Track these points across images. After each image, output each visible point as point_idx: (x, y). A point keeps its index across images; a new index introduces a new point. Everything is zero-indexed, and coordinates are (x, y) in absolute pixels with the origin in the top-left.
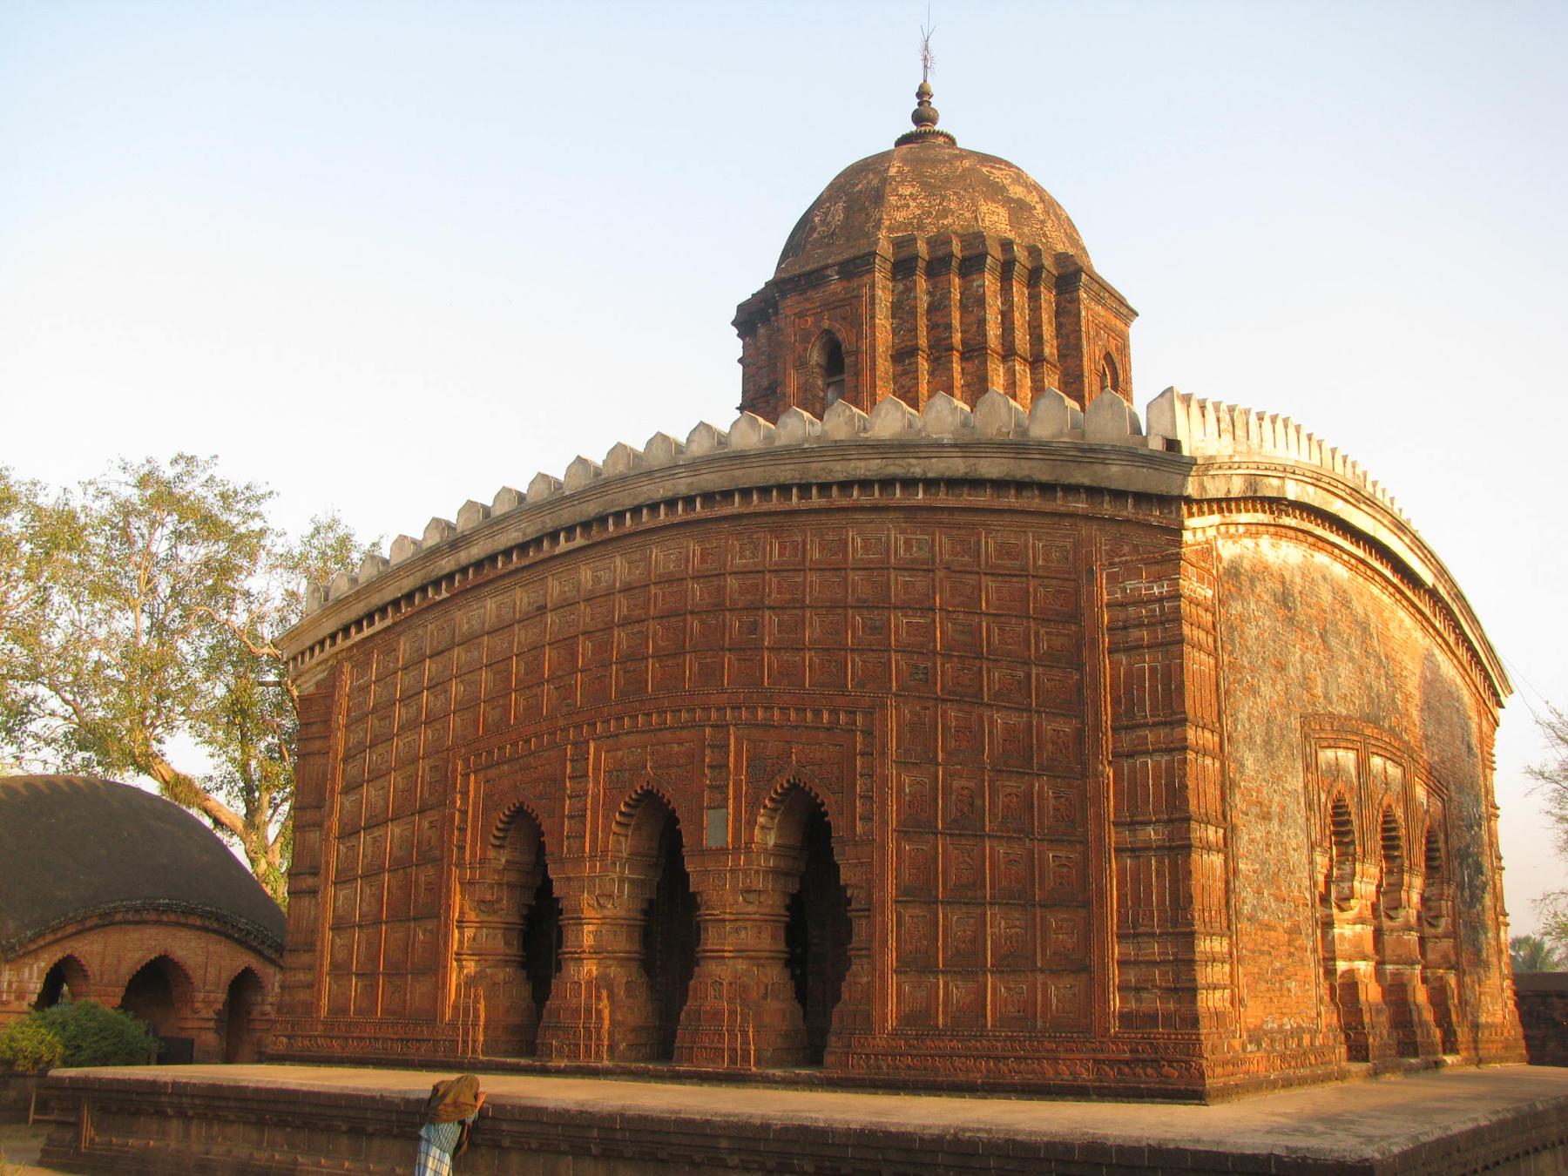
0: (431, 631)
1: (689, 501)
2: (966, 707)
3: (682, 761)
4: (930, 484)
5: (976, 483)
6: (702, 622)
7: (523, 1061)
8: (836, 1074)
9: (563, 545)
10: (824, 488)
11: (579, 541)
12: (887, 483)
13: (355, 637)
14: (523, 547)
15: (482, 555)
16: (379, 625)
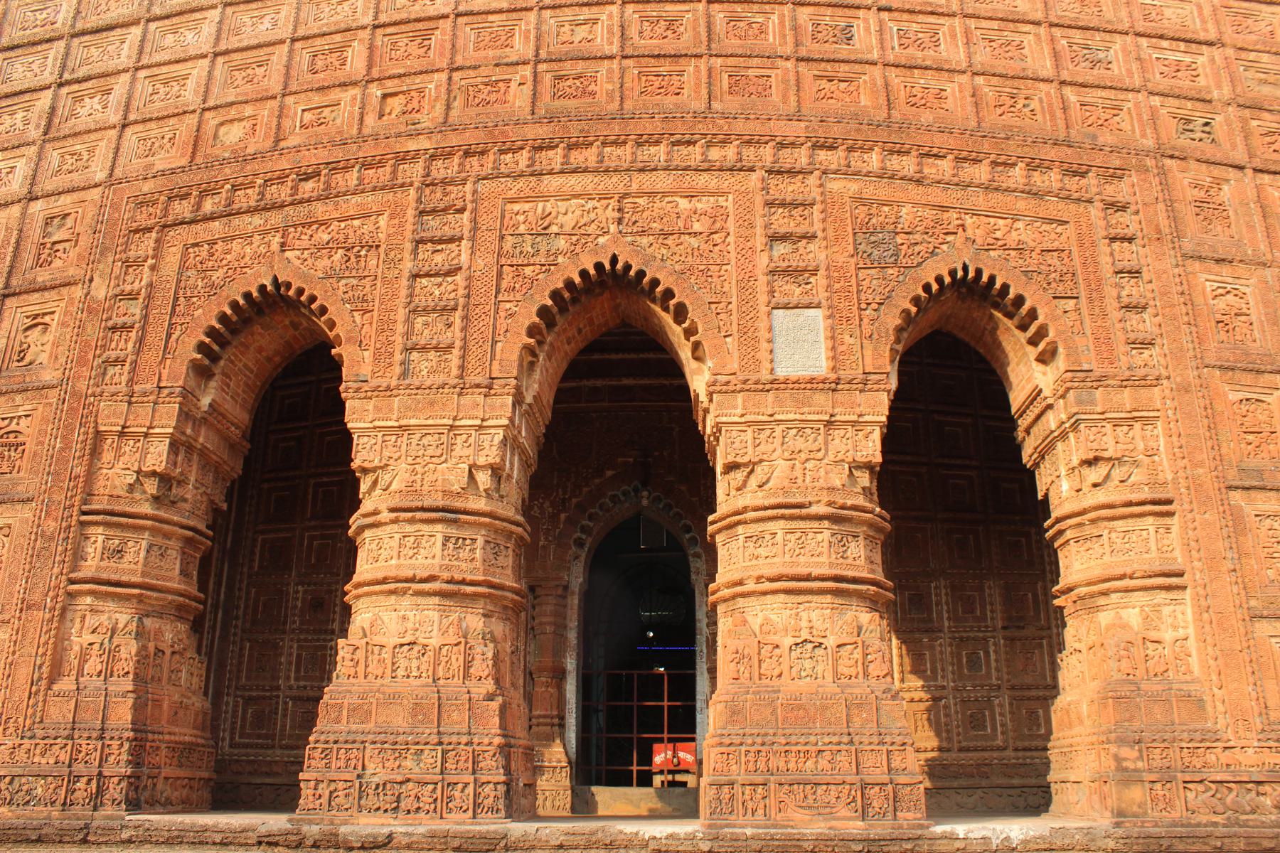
3: (697, 227)
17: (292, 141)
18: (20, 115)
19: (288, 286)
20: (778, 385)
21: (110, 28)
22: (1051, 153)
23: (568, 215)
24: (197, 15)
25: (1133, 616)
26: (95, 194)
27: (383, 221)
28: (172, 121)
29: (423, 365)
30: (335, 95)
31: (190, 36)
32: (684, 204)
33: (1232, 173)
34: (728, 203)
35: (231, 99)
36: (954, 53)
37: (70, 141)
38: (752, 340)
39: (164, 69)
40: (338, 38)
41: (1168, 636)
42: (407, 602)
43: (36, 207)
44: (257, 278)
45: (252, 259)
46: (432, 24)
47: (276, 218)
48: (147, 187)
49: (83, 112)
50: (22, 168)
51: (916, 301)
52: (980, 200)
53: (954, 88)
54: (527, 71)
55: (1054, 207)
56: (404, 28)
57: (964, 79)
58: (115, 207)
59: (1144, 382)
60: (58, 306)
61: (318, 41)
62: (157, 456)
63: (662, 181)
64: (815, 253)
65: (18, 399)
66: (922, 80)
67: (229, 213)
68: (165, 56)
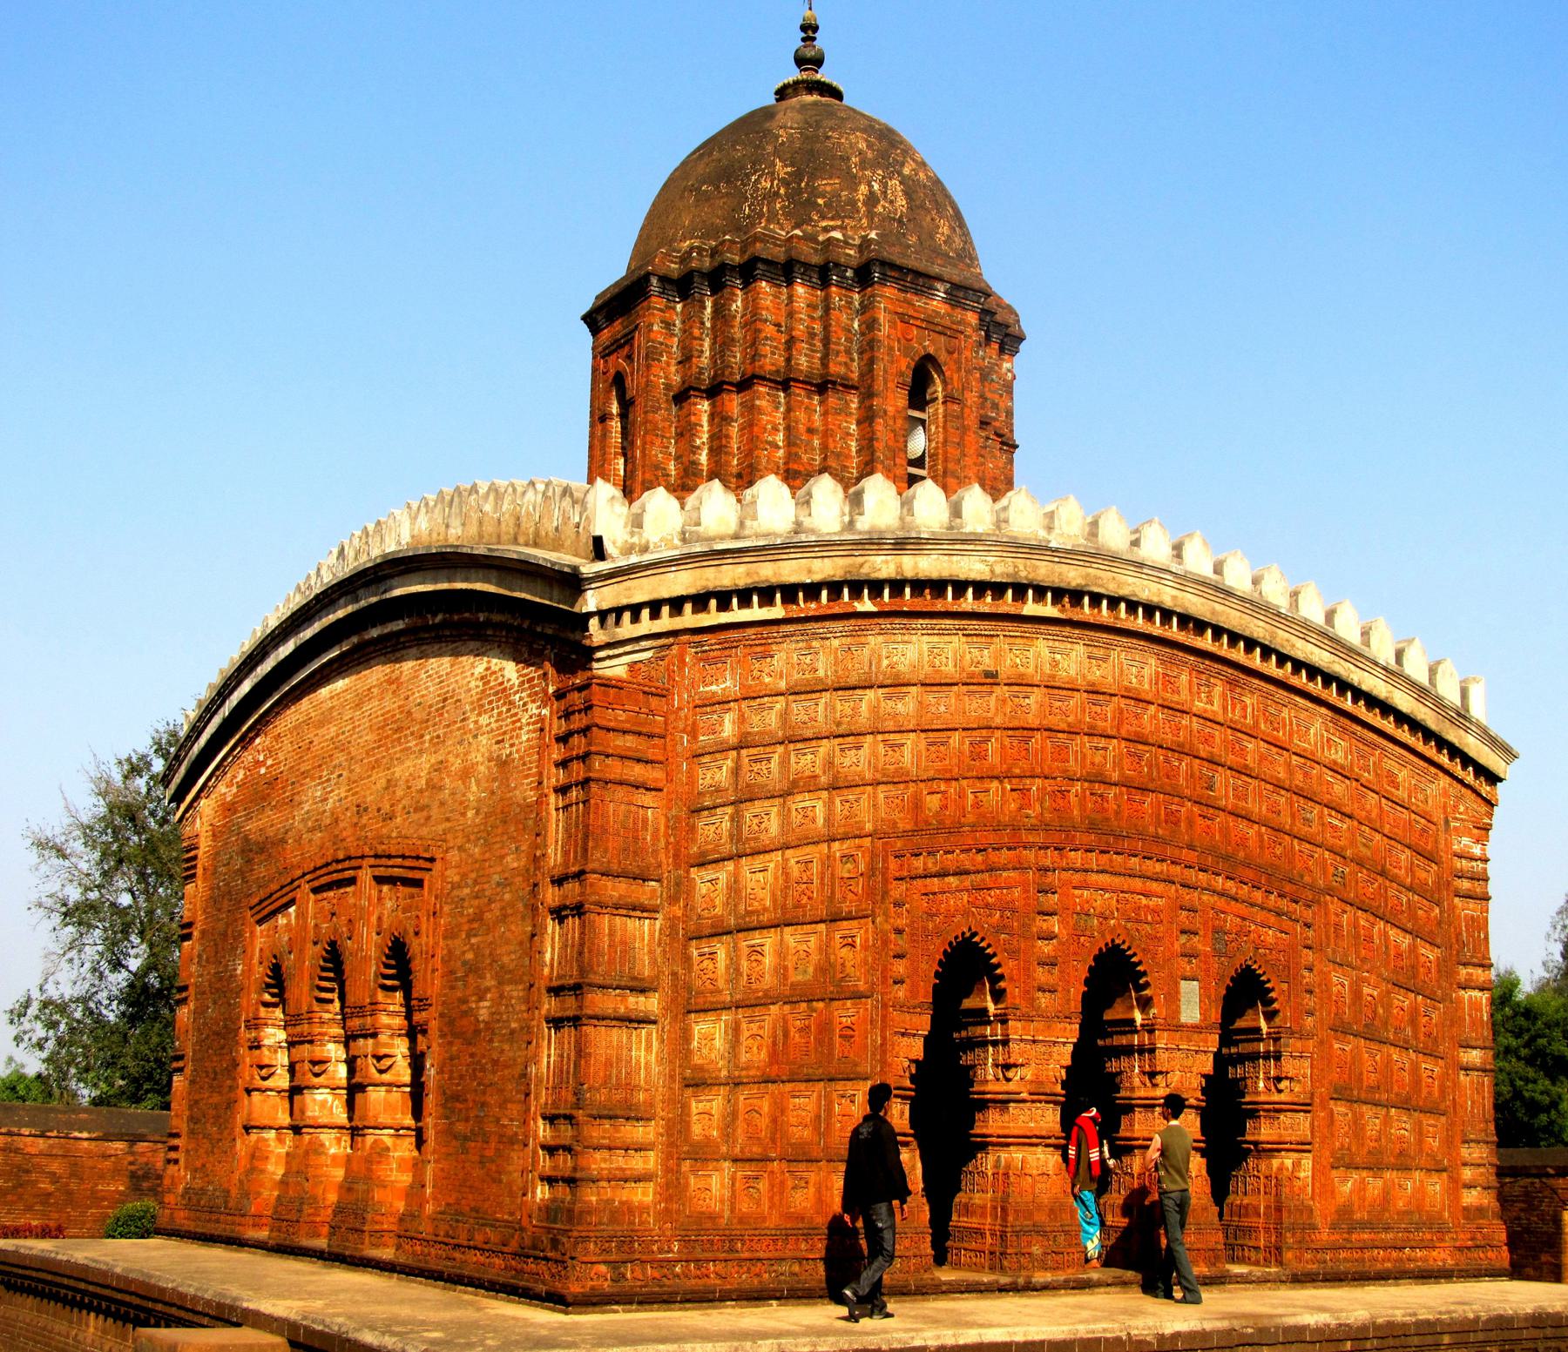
0: (825, 654)
1: (1167, 615)
2: (1371, 918)
4: (1358, 694)
5: (1386, 709)
6: (1167, 761)
7: (986, 1278)
8: (1300, 1268)
9: (1030, 608)
10: (1283, 659)
11: (1048, 610)
12: (1329, 678)
13: (713, 617)
14: (981, 588)
15: (935, 575)
16: (756, 613)
17: (971, 818)
18: (809, 757)
19: (975, 934)
20: (1180, 1027)
21: (854, 688)
22: (1288, 888)
23: (1100, 901)
24: (904, 689)
25: (1288, 1163)
26: (867, 842)
27: (1017, 892)
28: (902, 786)
29: (1044, 1000)
30: (986, 784)
31: (900, 707)
32: (1144, 901)
33: (1348, 908)
34: (1161, 902)
35: (931, 774)
36: (1254, 806)
37: (845, 792)
38: (1173, 997)
39: (892, 736)
40: (984, 732)
41: (1302, 1175)
42: (1040, 1149)
43: (836, 845)
44: (960, 927)
45: (957, 907)
46: (1030, 733)
47: (968, 881)
48: (899, 844)
49: (847, 762)
50: (819, 805)
51: (1232, 979)
52: (1260, 916)
53: (1252, 831)
54: (1078, 786)
55: (1286, 923)
56: (1017, 733)
57: (1256, 827)
58: (885, 860)
59: (1310, 1036)
60: (861, 932)
61: (975, 733)
62: (917, 1049)
63: (1138, 884)
64: (1199, 944)
65: (849, 1003)
66: (1242, 825)
67: (942, 874)
68: (890, 725)
